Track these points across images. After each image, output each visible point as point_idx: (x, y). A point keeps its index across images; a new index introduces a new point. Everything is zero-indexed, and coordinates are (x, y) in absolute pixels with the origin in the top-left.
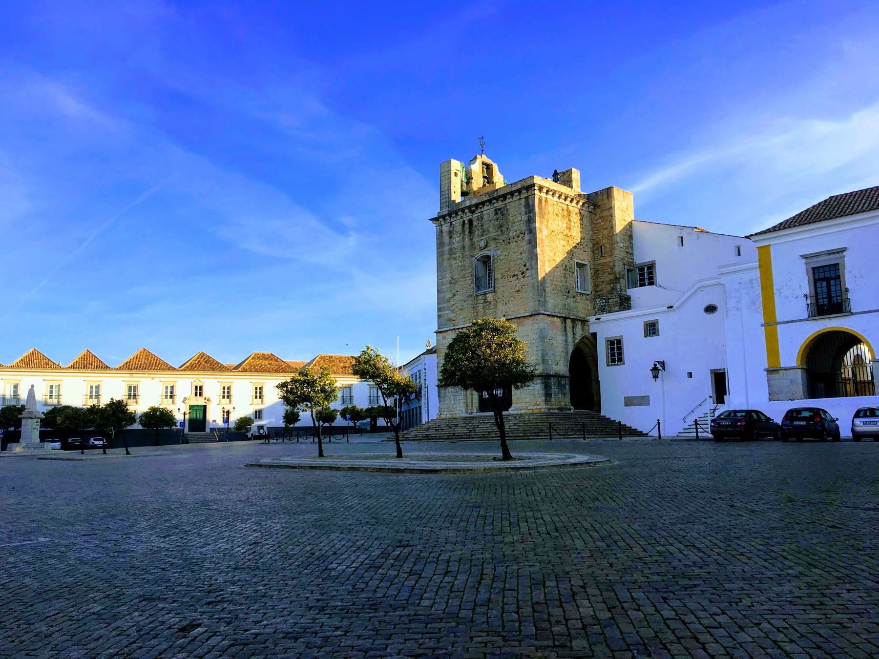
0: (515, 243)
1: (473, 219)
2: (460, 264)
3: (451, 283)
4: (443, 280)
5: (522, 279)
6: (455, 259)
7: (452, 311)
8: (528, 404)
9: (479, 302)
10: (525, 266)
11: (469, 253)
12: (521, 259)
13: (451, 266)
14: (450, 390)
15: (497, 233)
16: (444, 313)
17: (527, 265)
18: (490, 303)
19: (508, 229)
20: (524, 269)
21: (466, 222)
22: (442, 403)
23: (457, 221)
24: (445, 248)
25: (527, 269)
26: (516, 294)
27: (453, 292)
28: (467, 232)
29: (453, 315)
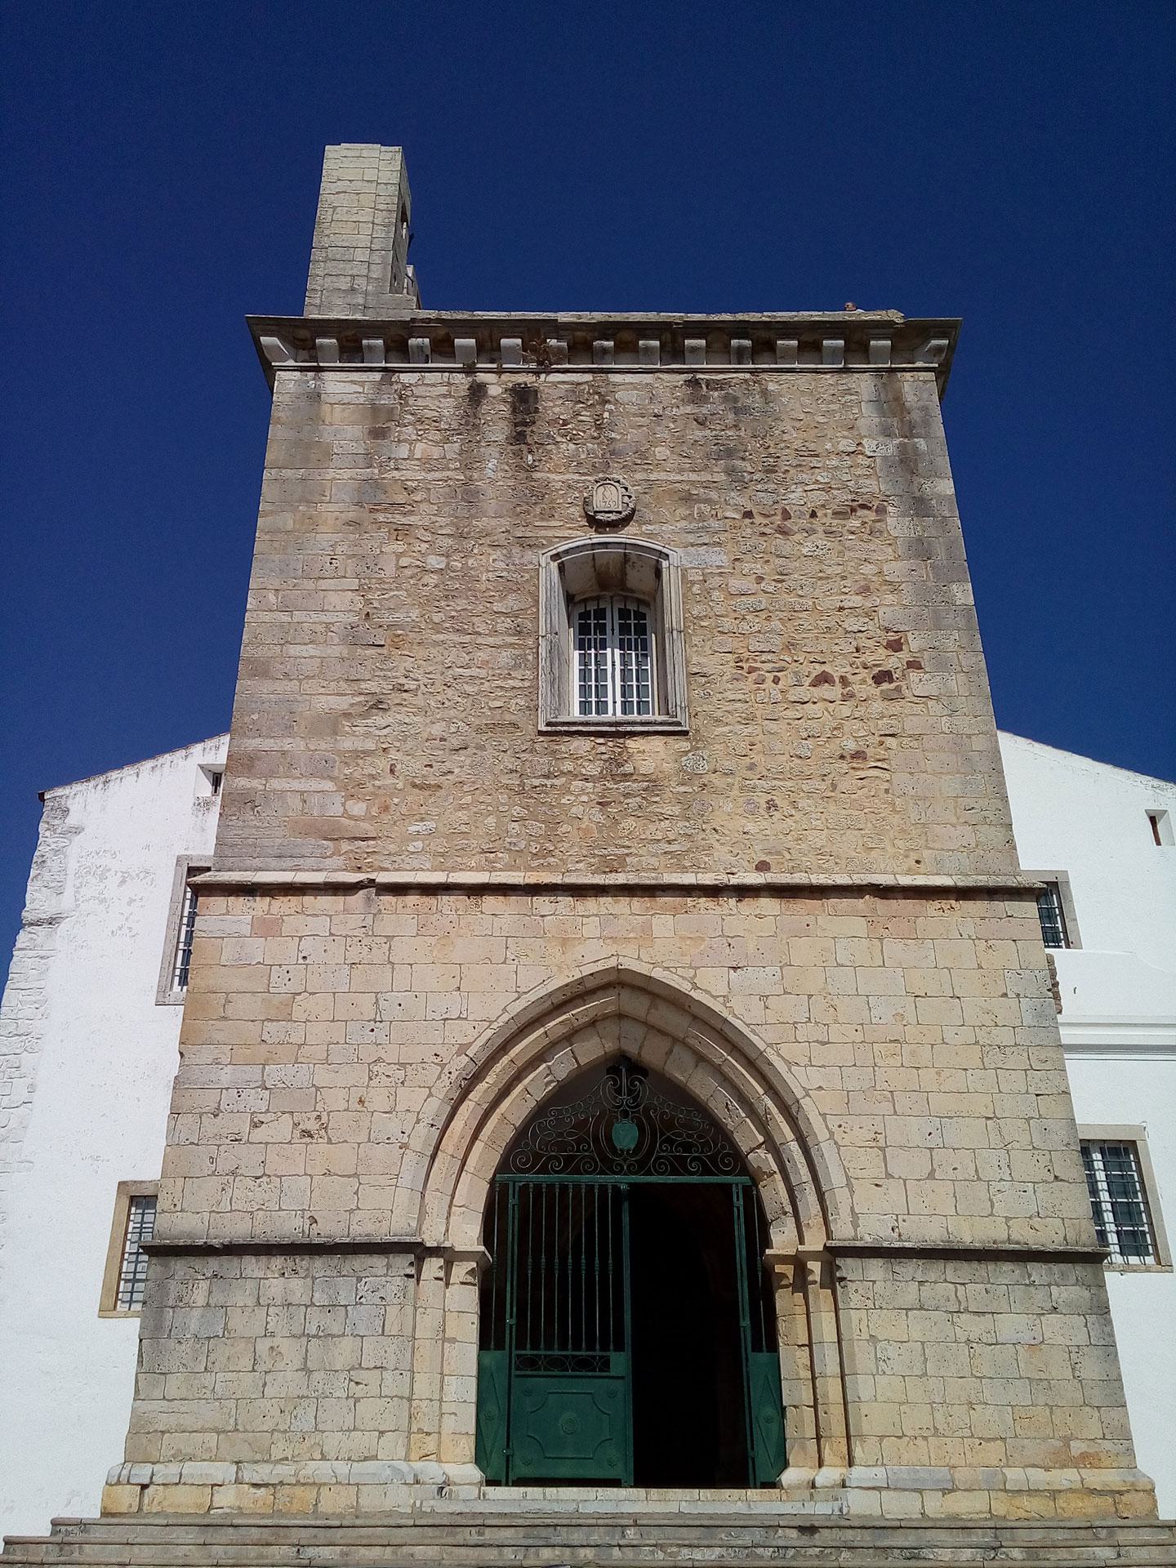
0: (820, 539)
1: (545, 391)
2: (435, 562)
3: (353, 638)
4: (298, 616)
5: (878, 706)
6: (401, 532)
7: (352, 789)
8: (994, 1452)
9: (568, 766)
10: (896, 646)
11: (505, 522)
12: (870, 614)
13: (368, 563)
14: (275, 1287)
15: (705, 477)
16: (276, 784)
17: (914, 643)
18: (653, 785)
19: (771, 470)
20: (893, 662)
21: (494, 391)
22: (174, 1385)
23: (430, 378)
24: (331, 474)
25: (914, 665)
26: (844, 766)
27: (372, 686)
28: (499, 431)
29: (358, 808)
